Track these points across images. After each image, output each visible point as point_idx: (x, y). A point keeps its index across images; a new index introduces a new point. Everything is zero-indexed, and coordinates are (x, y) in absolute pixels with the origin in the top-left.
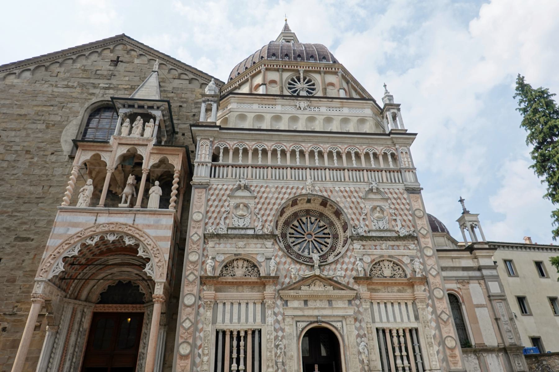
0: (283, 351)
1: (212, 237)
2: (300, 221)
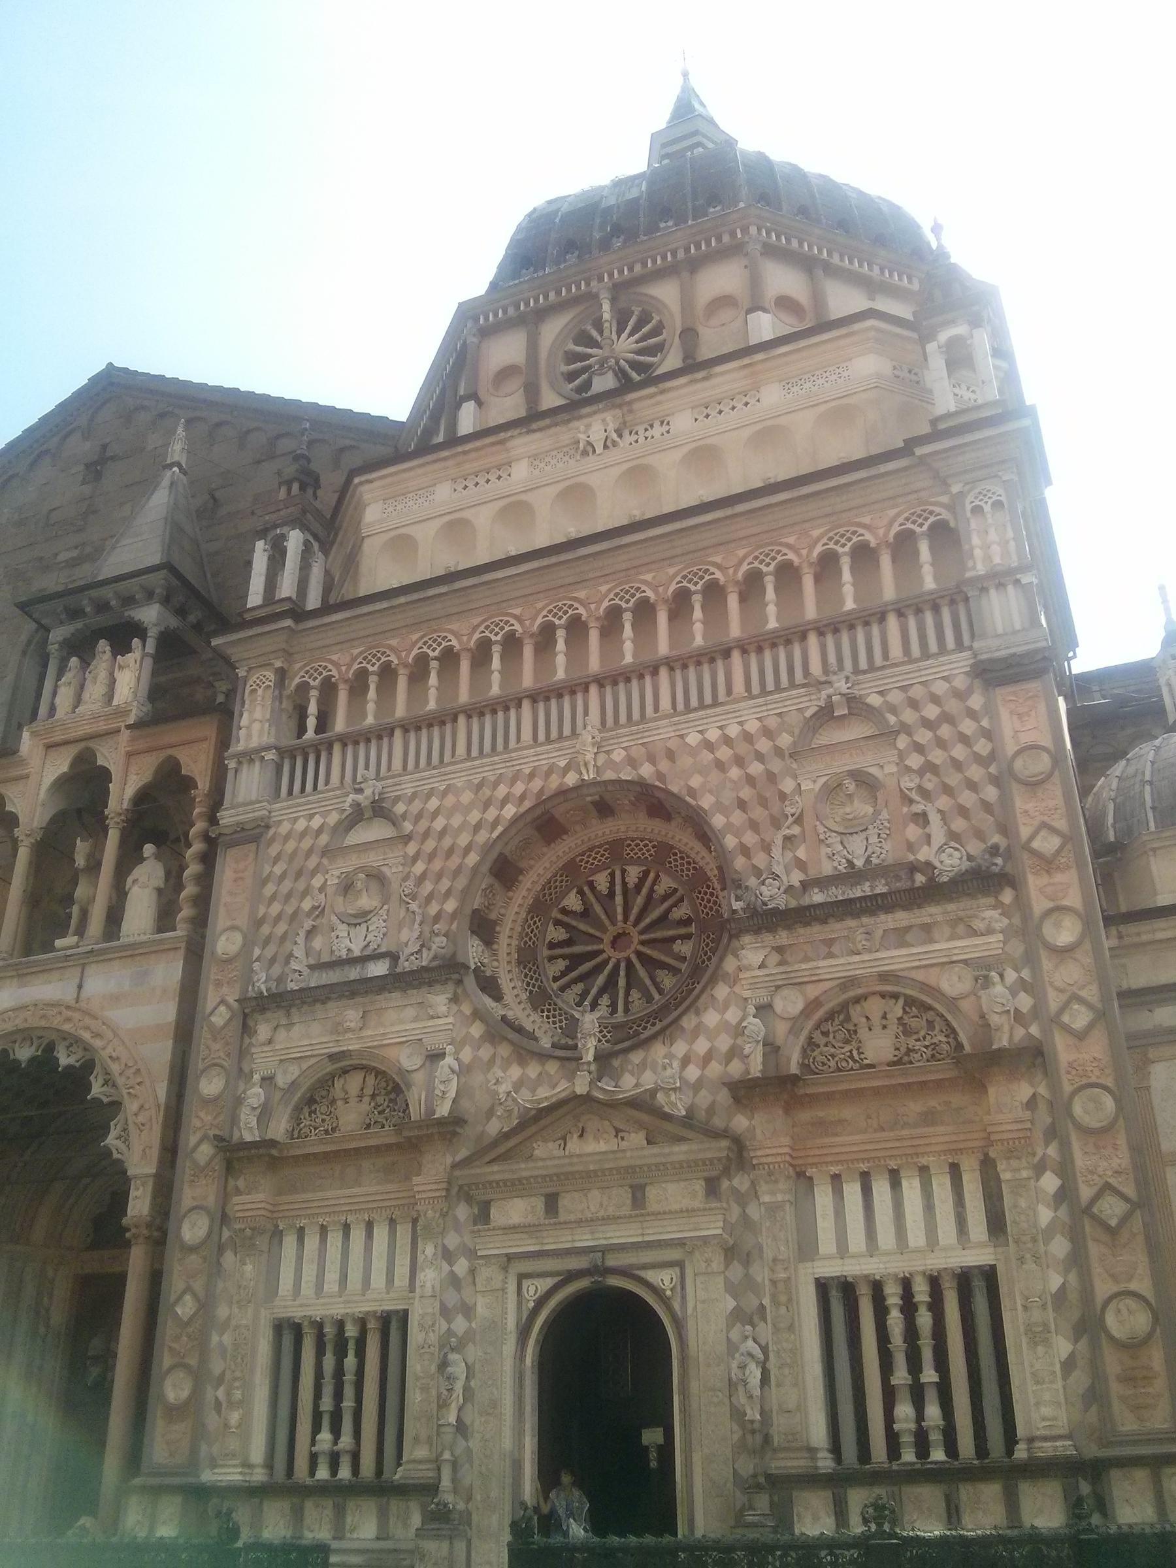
0: (459, 1386)
1: (264, 1009)
2: (586, 889)
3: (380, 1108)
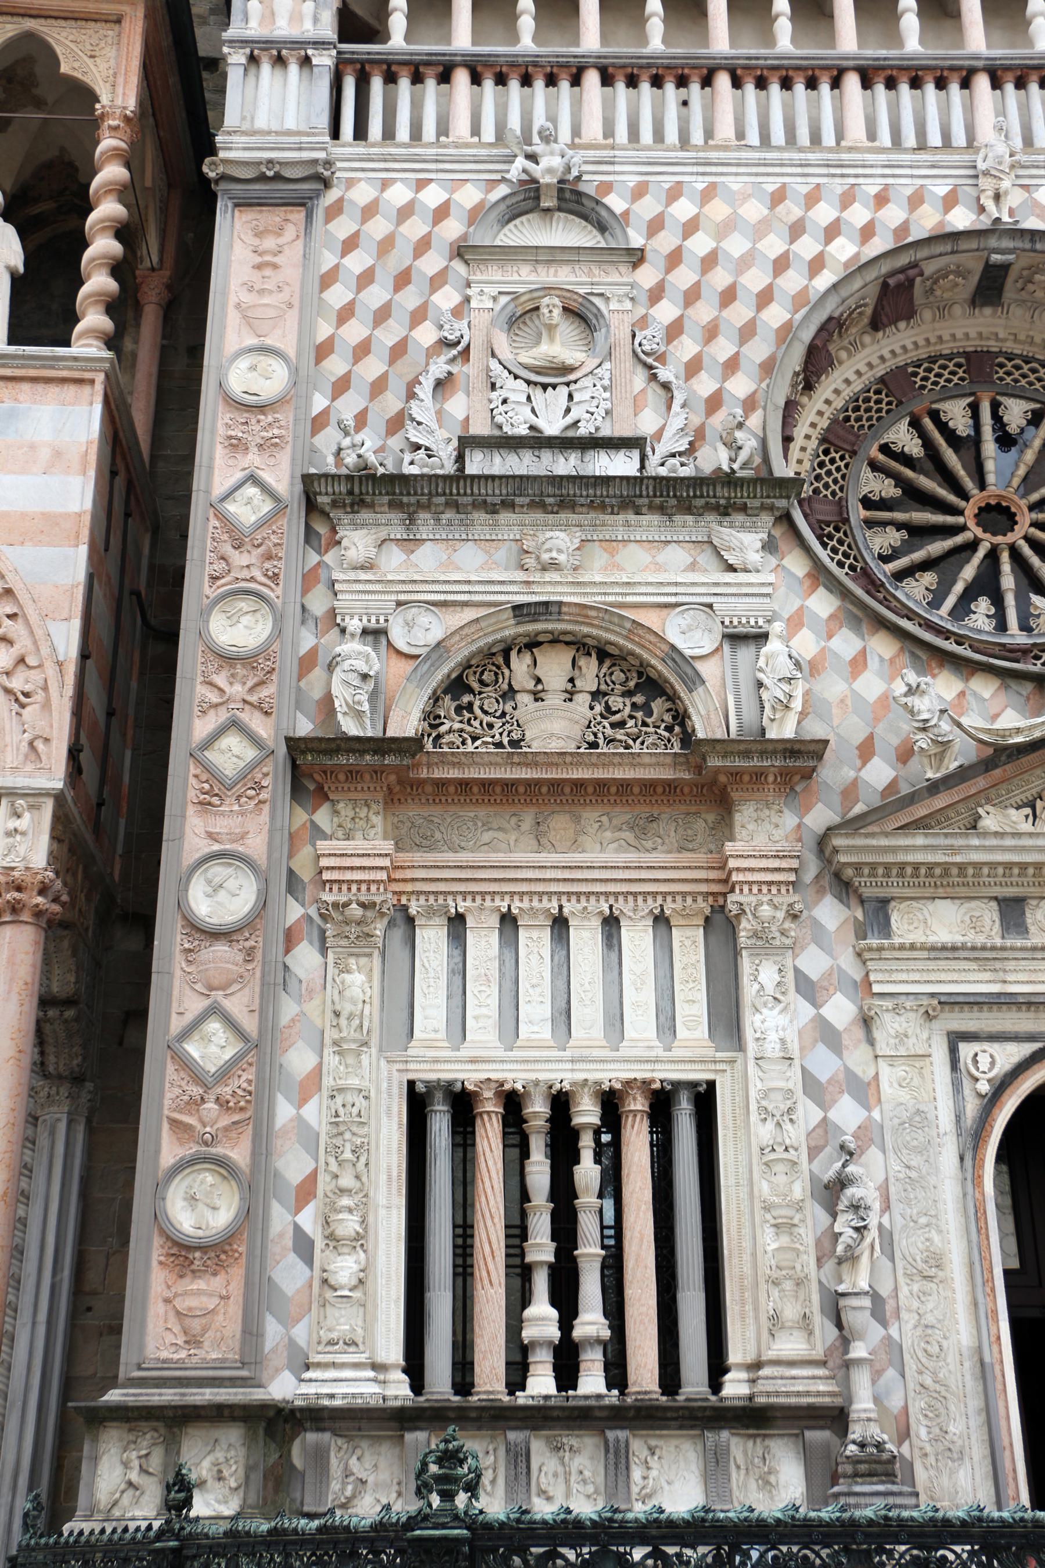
2: (927, 422)
3: (617, 718)
